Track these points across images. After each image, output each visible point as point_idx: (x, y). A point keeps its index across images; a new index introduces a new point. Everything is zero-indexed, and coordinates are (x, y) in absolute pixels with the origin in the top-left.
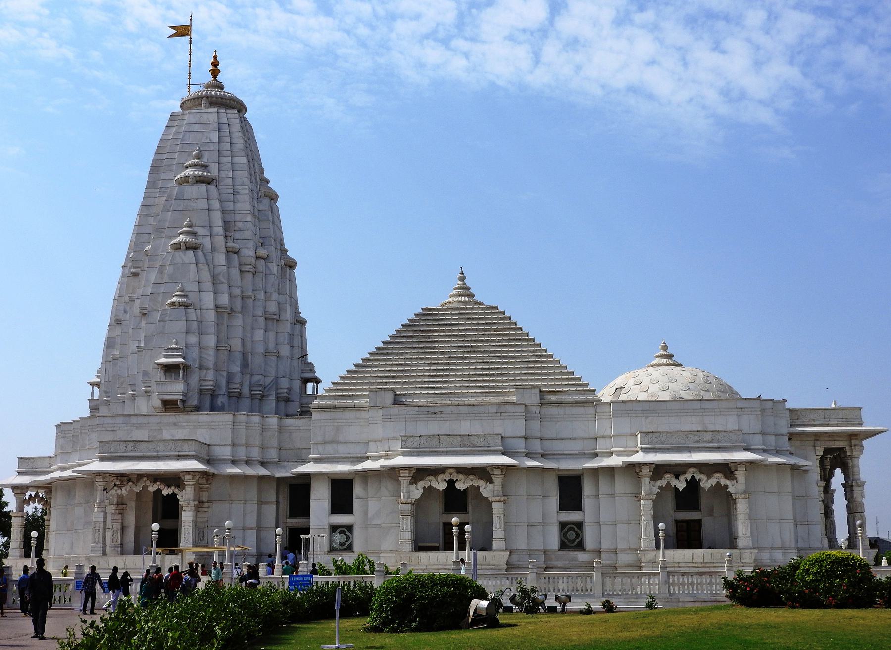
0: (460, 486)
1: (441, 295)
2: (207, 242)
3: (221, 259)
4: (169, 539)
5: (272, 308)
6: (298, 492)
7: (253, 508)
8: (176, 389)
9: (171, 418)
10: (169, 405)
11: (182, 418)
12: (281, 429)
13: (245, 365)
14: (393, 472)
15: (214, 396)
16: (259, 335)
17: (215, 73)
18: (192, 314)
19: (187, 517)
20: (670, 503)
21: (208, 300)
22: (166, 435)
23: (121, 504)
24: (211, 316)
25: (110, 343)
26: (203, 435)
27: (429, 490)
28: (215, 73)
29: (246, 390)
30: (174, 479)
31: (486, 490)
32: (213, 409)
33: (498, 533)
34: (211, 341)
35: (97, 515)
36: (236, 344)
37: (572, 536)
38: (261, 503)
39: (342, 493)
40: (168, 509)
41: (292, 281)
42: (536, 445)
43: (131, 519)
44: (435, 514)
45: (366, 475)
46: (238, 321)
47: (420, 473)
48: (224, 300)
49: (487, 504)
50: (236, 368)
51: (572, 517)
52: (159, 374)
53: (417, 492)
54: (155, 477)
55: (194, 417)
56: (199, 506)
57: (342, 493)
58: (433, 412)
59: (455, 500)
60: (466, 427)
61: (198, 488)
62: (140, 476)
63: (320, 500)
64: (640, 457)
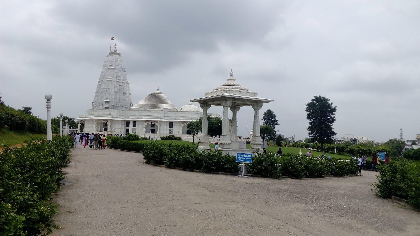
0: (153, 123)
1: (154, 91)
2: (113, 80)
3: (116, 83)
4: (106, 130)
5: (125, 92)
6: (128, 123)
7: (120, 125)
8: (107, 105)
9: (106, 110)
10: (106, 108)
11: (108, 110)
12: (125, 113)
13: (120, 101)
14: (142, 121)
15: (114, 106)
16: (122, 96)
17: (115, 47)
18: (111, 93)
19: (109, 126)
20: (186, 127)
21: (113, 90)
22: (106, 113)
23: (98, 124)
24: (114, 93)
25: (96, 96)
26: (112, 113)
27: (148, 124)
28: (115, 47)
29: (120, 106)
30: (107, 120)
31: (157, 124)
32: (114, 109)
33: (158, 131)
34: (114, 97)
35: (94, 126)
36: (118, 98)
37: (171, 132)
38: (121, 124)
39: (135, 124)
40: (106, 125)
41: (129, 87)
42: (166, 118)
43: (99, 126)
44: (150, 128)
45: (139, 121)
46: (119, 94)
47: (146, 121)
48: (116, 90)
49: (157, 126)
50: (118, 102)
51: (171, 129)
52: (104, 103)
53: (146, 124)
54: (104, 120)
55: (110, 110)
56: (111, 124)
57: (135, 124)
58: (150, 111)
59: (153, 125)
60: (155, 114)
61: (111, 122)
62: (101, 119)
63: (131, 125)
64: (180, 120)
